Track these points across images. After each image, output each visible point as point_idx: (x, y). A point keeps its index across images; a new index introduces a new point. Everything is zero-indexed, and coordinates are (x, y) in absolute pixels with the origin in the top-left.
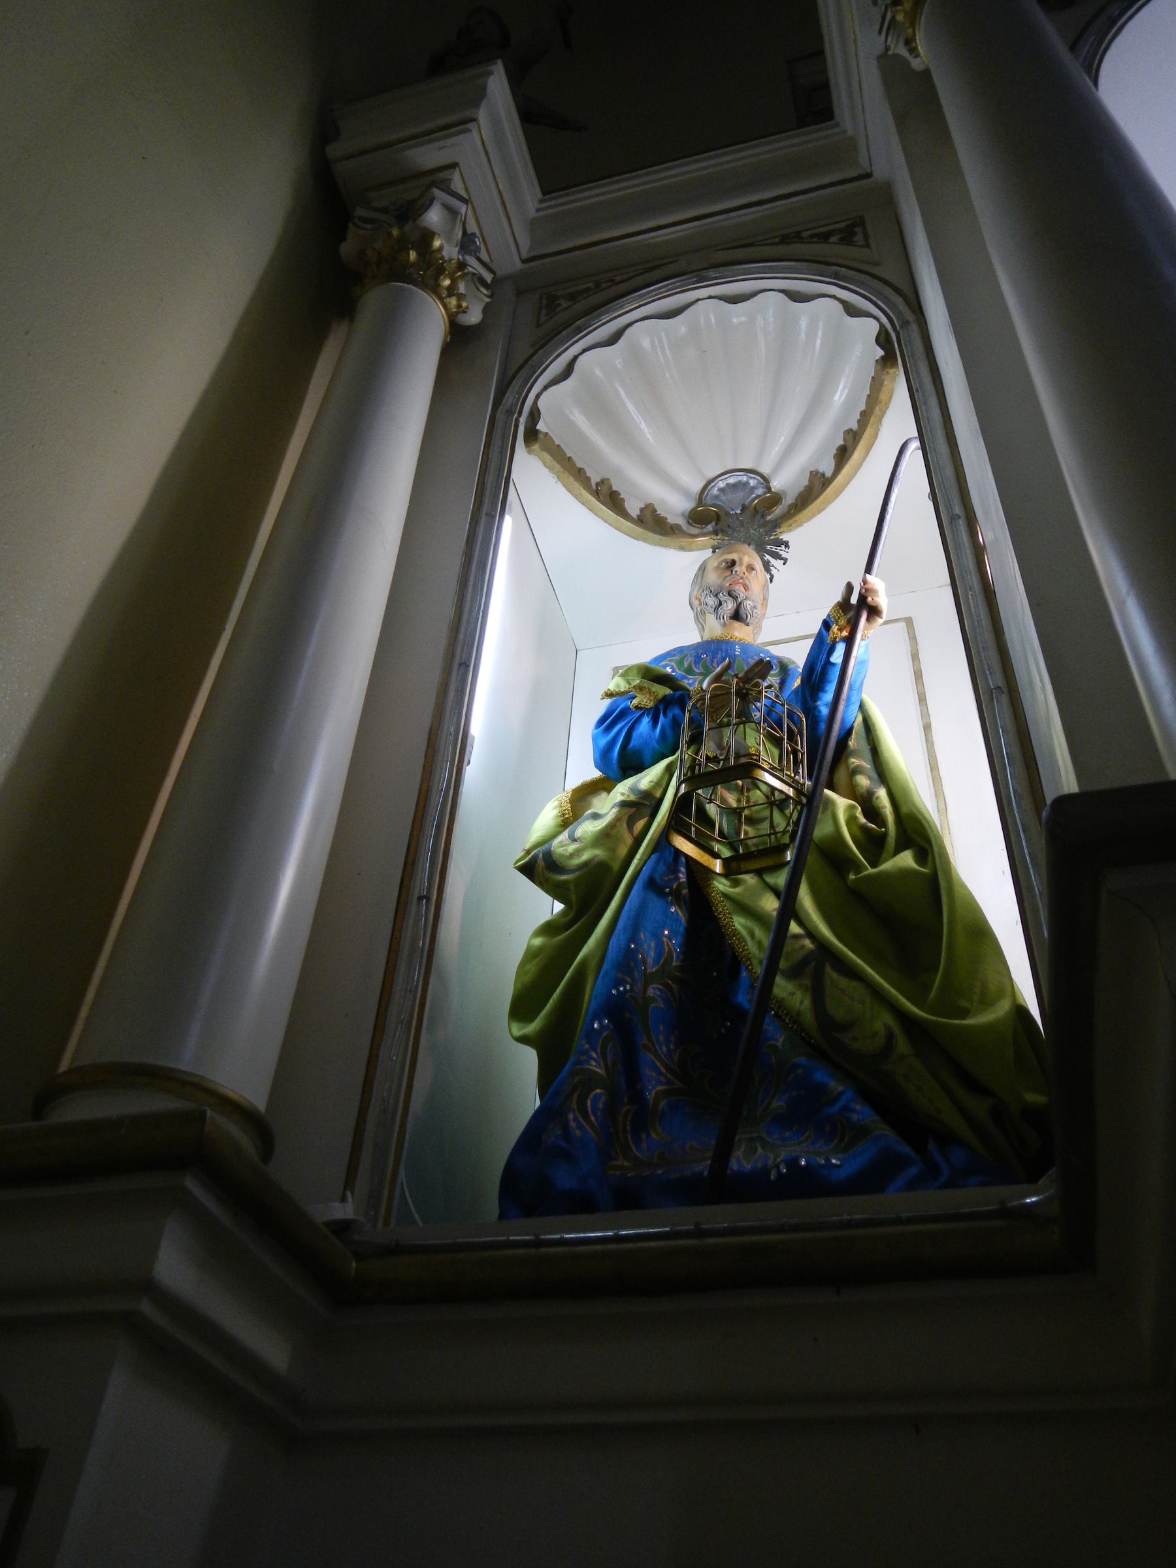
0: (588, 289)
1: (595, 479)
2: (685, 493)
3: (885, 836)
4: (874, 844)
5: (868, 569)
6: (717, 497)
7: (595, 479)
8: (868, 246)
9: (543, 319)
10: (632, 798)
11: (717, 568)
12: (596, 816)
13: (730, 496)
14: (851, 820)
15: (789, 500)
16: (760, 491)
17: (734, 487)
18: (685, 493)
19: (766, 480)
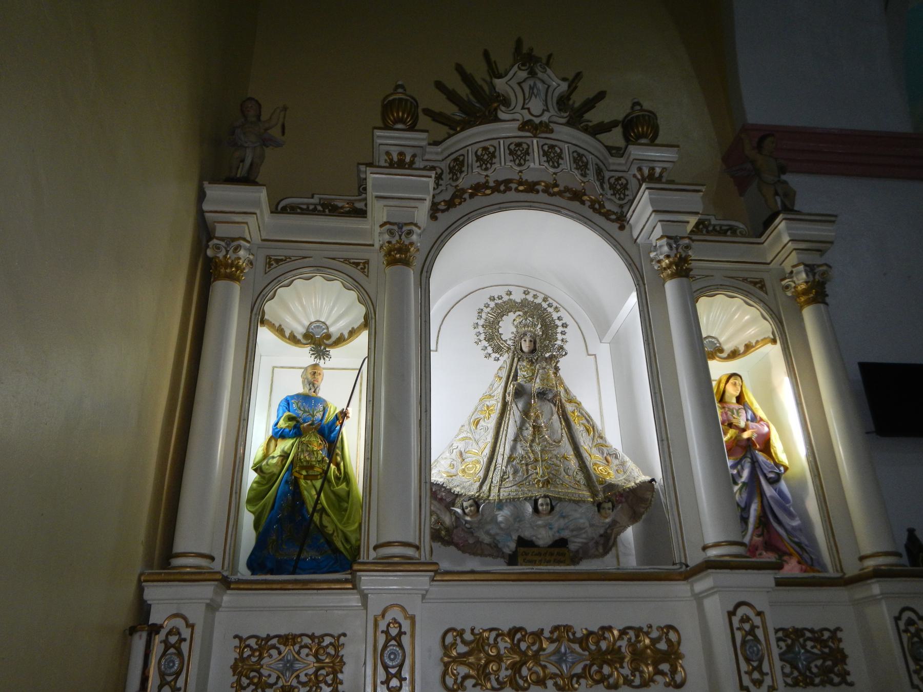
0: (282, 260)
1: (277, 325)
2: (303, 326)
3: (340, 478)
4: (337, 478)
5: (348, 406)
6: (312, 329)
7: (277, 325)
8: (368, 276)
9: (267, 270)
10: (283, 454)
11: (310, 373)
12: (273, 457)
13: (317, 330)
14: (334, 472)
15: (333, 339)
16: (325, 331)
17: (318, 327)
18: (303, 326)
19: (328, 328)
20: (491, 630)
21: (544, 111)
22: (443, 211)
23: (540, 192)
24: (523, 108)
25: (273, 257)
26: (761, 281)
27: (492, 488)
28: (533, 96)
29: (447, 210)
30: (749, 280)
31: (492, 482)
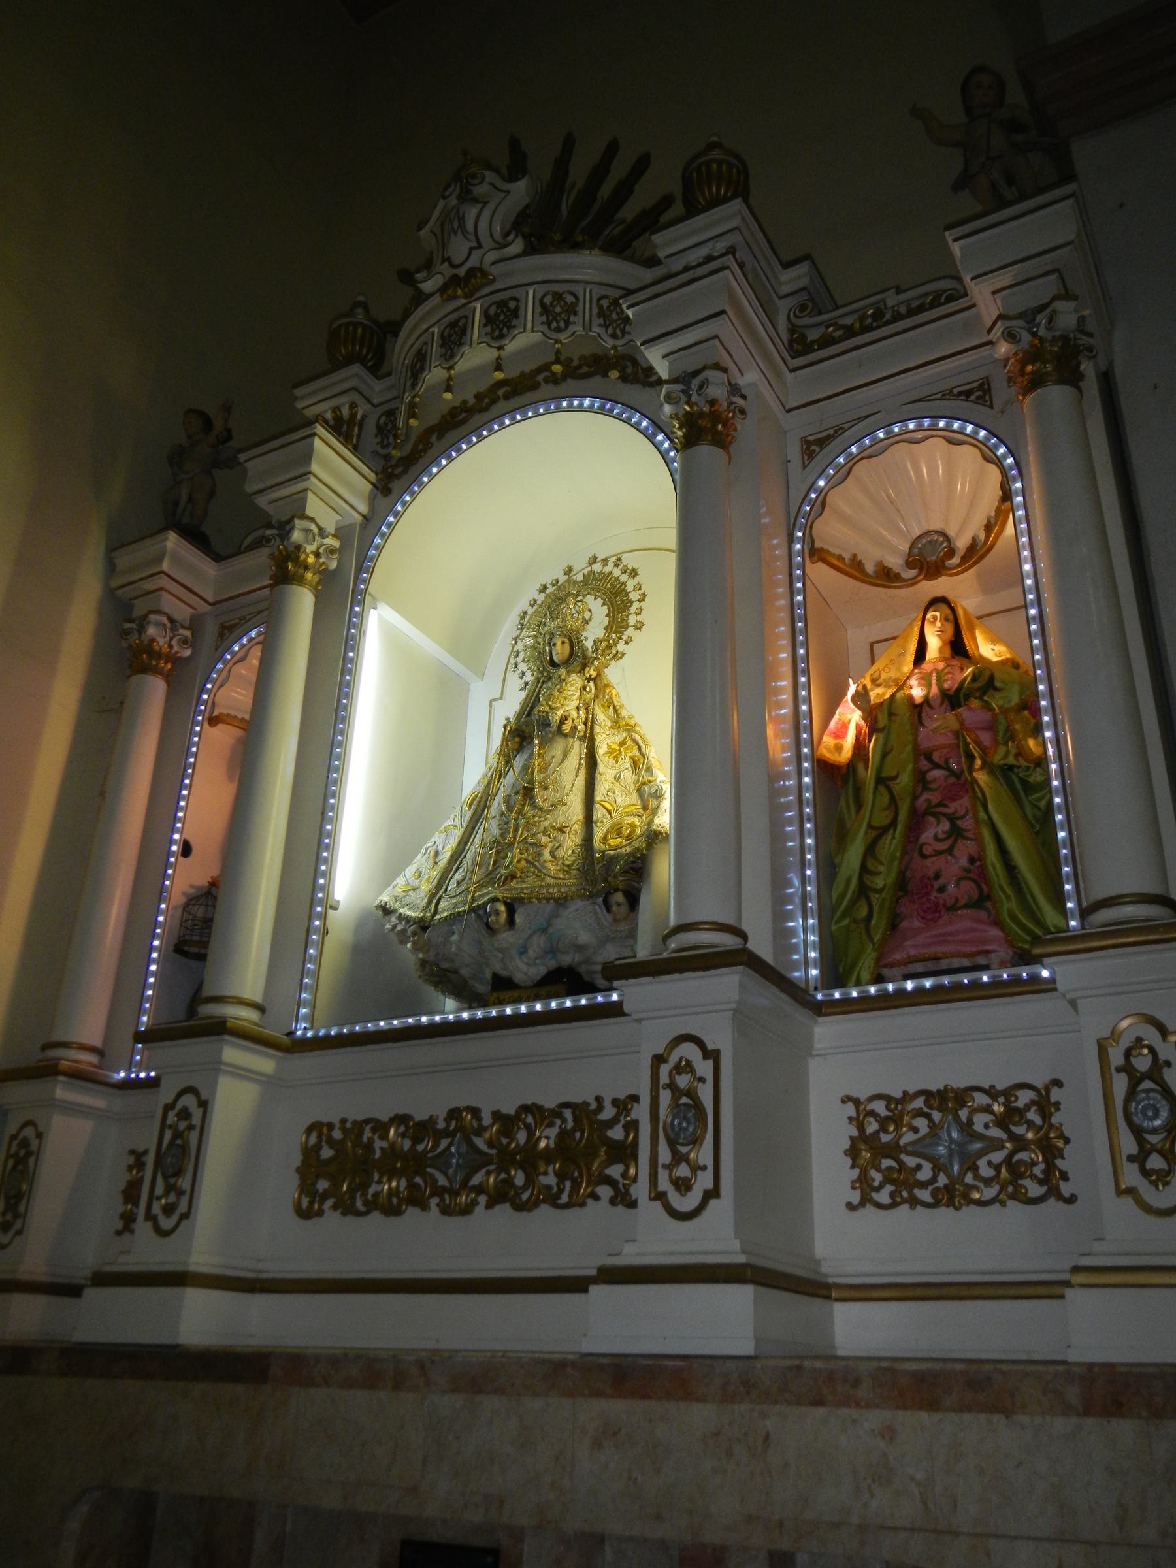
20: (367, 1121)
21: (471, 249)
22: (398, 477)
23: (542, 383)
24: (443, 261)
25: (227, 624)
26: (981, 386)
27: (443, 899)
28: (452, 234)
29: (405, 472)
30: (955, 391)
31: (446, 890)
